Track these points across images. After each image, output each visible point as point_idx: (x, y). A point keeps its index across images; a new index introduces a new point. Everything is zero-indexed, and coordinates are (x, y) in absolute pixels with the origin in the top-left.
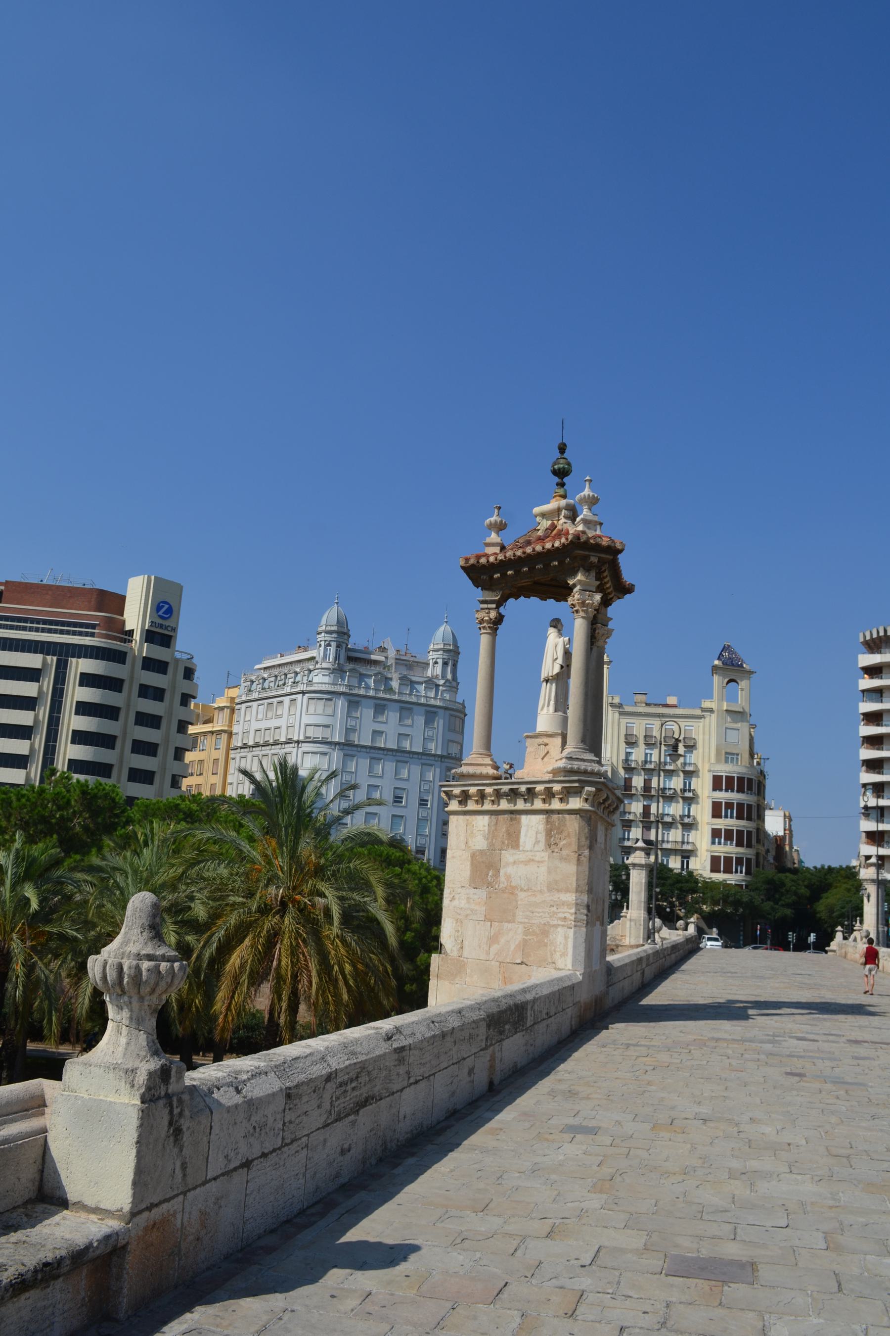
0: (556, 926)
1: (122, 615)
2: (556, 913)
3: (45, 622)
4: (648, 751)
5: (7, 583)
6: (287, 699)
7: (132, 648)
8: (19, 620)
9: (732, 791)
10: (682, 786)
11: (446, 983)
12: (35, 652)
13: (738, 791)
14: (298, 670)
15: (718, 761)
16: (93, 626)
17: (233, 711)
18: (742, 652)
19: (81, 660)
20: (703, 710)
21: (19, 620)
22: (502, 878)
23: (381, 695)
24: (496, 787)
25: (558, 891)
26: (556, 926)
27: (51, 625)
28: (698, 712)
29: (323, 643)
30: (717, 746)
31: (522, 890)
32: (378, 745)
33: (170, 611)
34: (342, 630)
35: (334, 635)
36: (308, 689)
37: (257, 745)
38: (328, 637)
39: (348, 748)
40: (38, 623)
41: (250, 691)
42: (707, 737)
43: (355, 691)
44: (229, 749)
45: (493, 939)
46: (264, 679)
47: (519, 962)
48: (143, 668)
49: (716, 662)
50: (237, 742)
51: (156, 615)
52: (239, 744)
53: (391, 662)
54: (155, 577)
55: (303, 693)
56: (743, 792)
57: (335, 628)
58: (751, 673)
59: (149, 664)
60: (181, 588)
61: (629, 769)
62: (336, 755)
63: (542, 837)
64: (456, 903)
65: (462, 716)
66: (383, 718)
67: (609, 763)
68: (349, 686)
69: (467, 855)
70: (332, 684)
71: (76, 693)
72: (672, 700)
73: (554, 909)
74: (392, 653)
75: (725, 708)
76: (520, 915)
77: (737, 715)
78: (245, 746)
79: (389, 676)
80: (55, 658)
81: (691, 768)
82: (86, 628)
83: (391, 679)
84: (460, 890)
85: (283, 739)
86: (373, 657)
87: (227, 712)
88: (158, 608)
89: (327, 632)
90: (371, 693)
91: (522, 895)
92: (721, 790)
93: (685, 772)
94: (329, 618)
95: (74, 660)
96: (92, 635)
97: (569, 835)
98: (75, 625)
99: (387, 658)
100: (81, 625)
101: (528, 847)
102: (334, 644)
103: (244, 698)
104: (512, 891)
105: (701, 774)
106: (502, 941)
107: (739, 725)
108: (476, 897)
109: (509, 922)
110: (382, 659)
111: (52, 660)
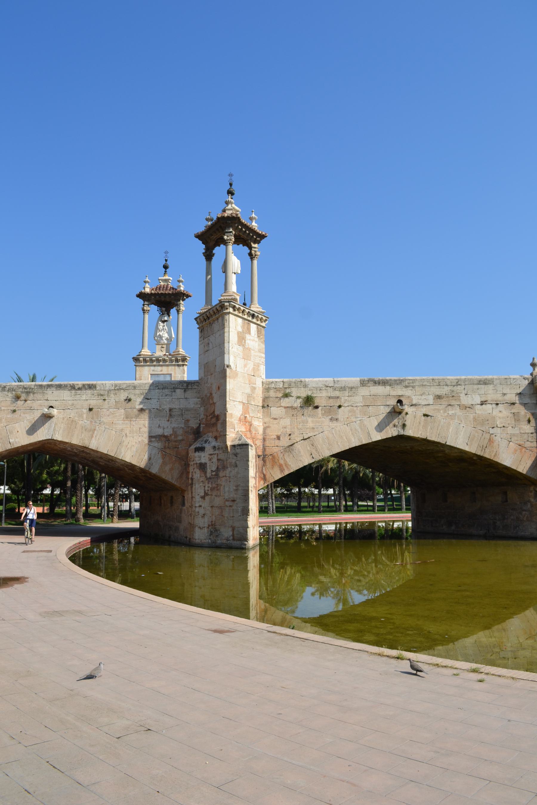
0: (261, 364)
2: (261, 360)
11: (232, 380)
22: (247, 344)
24: (245, 309)
25: (261, 353)
26: (261, 364)
31: (252, 350)
45: (245, 366)
47: (252, 375)
63: (256, 332)
64: (233, 349)
69: (236, 332)
73: (260, 358)
76: (252, 359)
84: (234, 345)
91: (252, 352)
97: (262, 335)
101: (253, 335)
104: (249, 349)
106: (248, 367)
108: (239, 349)
109: (249, 360)
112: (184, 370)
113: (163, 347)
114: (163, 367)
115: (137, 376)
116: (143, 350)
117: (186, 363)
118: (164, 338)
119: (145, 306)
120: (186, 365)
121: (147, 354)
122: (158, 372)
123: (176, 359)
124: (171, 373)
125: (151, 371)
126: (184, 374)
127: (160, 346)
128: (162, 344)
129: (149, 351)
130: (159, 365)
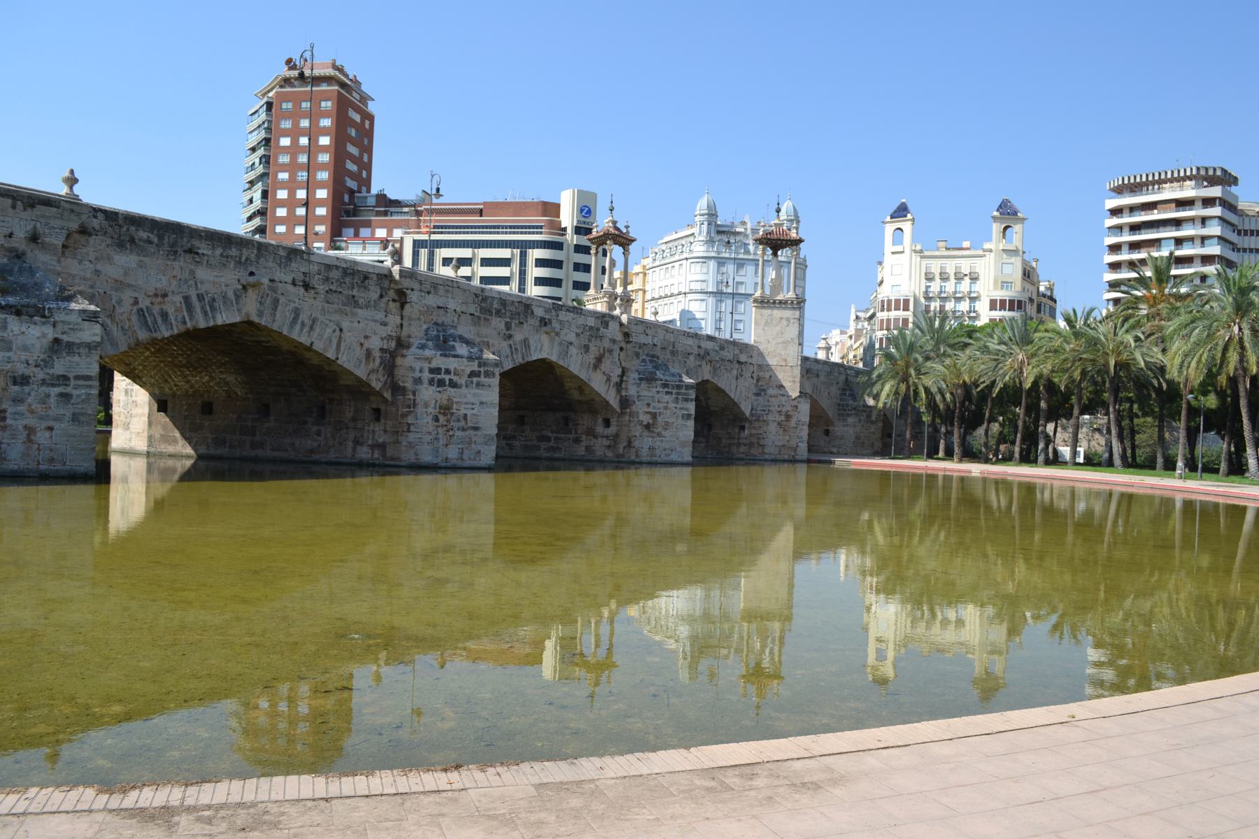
1: (559, 217)
3: (511, 227)
4: (943, 284)
5: (484, 204)
6: (677, 264)
7: (566, 240)
8: (495, 227)
9: (1005, 310)
10: (968, 309)
12: (506, 247)
13: (1009, 310)
14: (684, 243)
15: (995, 288)
16: (541, 227)
17: (645, 274)
18: (1017, 203)
19: (535, 250)
20: (984, 251)
21: (495, 227)
23: (741, 256)
27: (514, 228)
28: (980, 252)
29: (698, 223)
30: (995, 277)
32: (740, 291)
33: (589, 212)
34: (711, 212)
35: (706, 217)
36: (691, 256)
37: (661, 298)
38: (702, 218)
39: (719, 295)
40: (506, 228)
41: (655, 260)
42: (987, 271)
43: (723, 255)
44: (644, 302)
46: (664, 251)
48: (575, 252)
49: (996, 213)
50: (648, 297)
51: (580, 216)
52: (650, 298)
53: (749, 232)
54: (578, 191)
55: (687, 259)
56: (1014, 310)
57: (706, 212)
58: (1024, 219)
59: (580, 249)
60: (596, 195)
61: (928, 298)
62: (711, 300)
65: (804, 267)
66: (742, 272)
67: (913, 294)
68: (719, 252)
70: (707, 251)
71: (535, 272)
72: (966, 244)
74: (749, 226)
75: (1001, 248)
77: (1014, 252)
78: (653, 299)
79: (747, 242)
80: (519, 250)
81: (975, 295)
82: (536, 228)
83: (749, 244)
85: (676, 292)
86: (738, 230)
87: (641, 275)
88: (582, 211)
89: (701, 215)
90: (733, 256)
92: (996, 310)
93: (970, 298)
94: (702, 205)
95: (530, 250)
96: (541, 233)
98: (530, 227)
99: (746, 229)
100: (534, 227)
102: (706, 223)
103: (651, 265)
105: (982, 298)
107: (1013, 260)
110: (742, 230)
111: (517, 252)
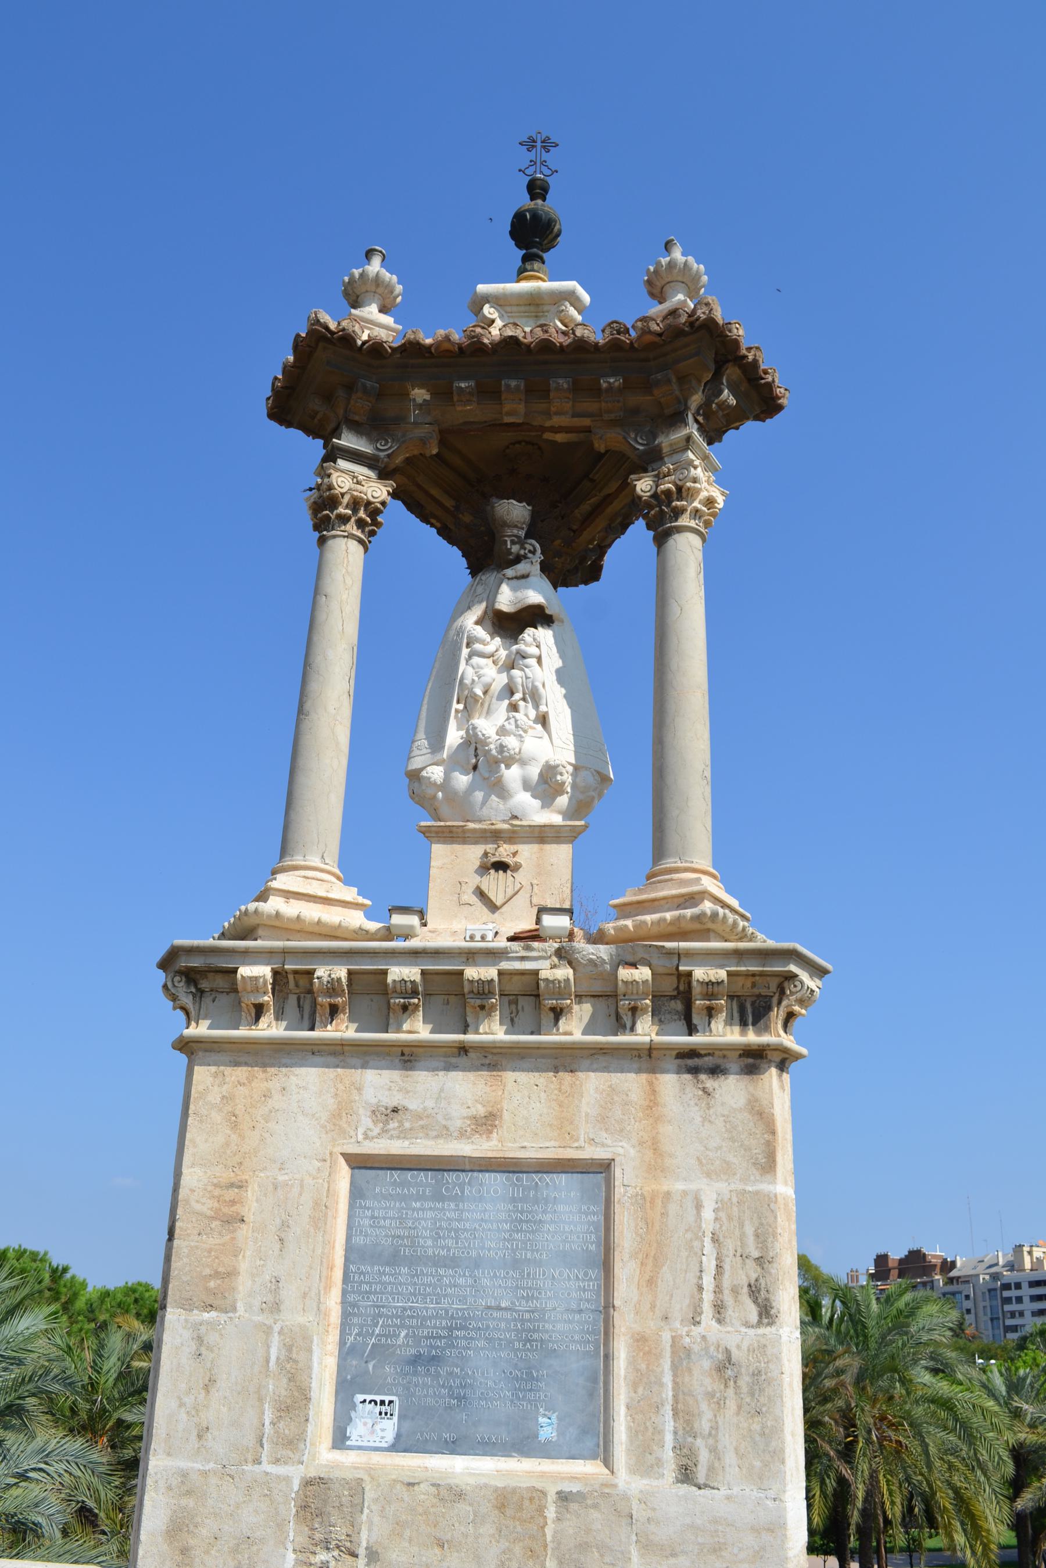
112: (764, 1118)
113: (501, 866)
114: (509, 1076)
115: (191, 1177)
116: (282, 882)
117: (776, 1036)
118: (512, 775)
119: (342, 463)
120: (784, 1060)
121: (333, 916)
122: (445, 1133)
123: (669, 986)
124: (600, 1154)
125: (366, 1122)
126: (768, 1165)
127: (474, 853)
128: (495, 836)
129: (350, 894)
130: (463, 1049)
